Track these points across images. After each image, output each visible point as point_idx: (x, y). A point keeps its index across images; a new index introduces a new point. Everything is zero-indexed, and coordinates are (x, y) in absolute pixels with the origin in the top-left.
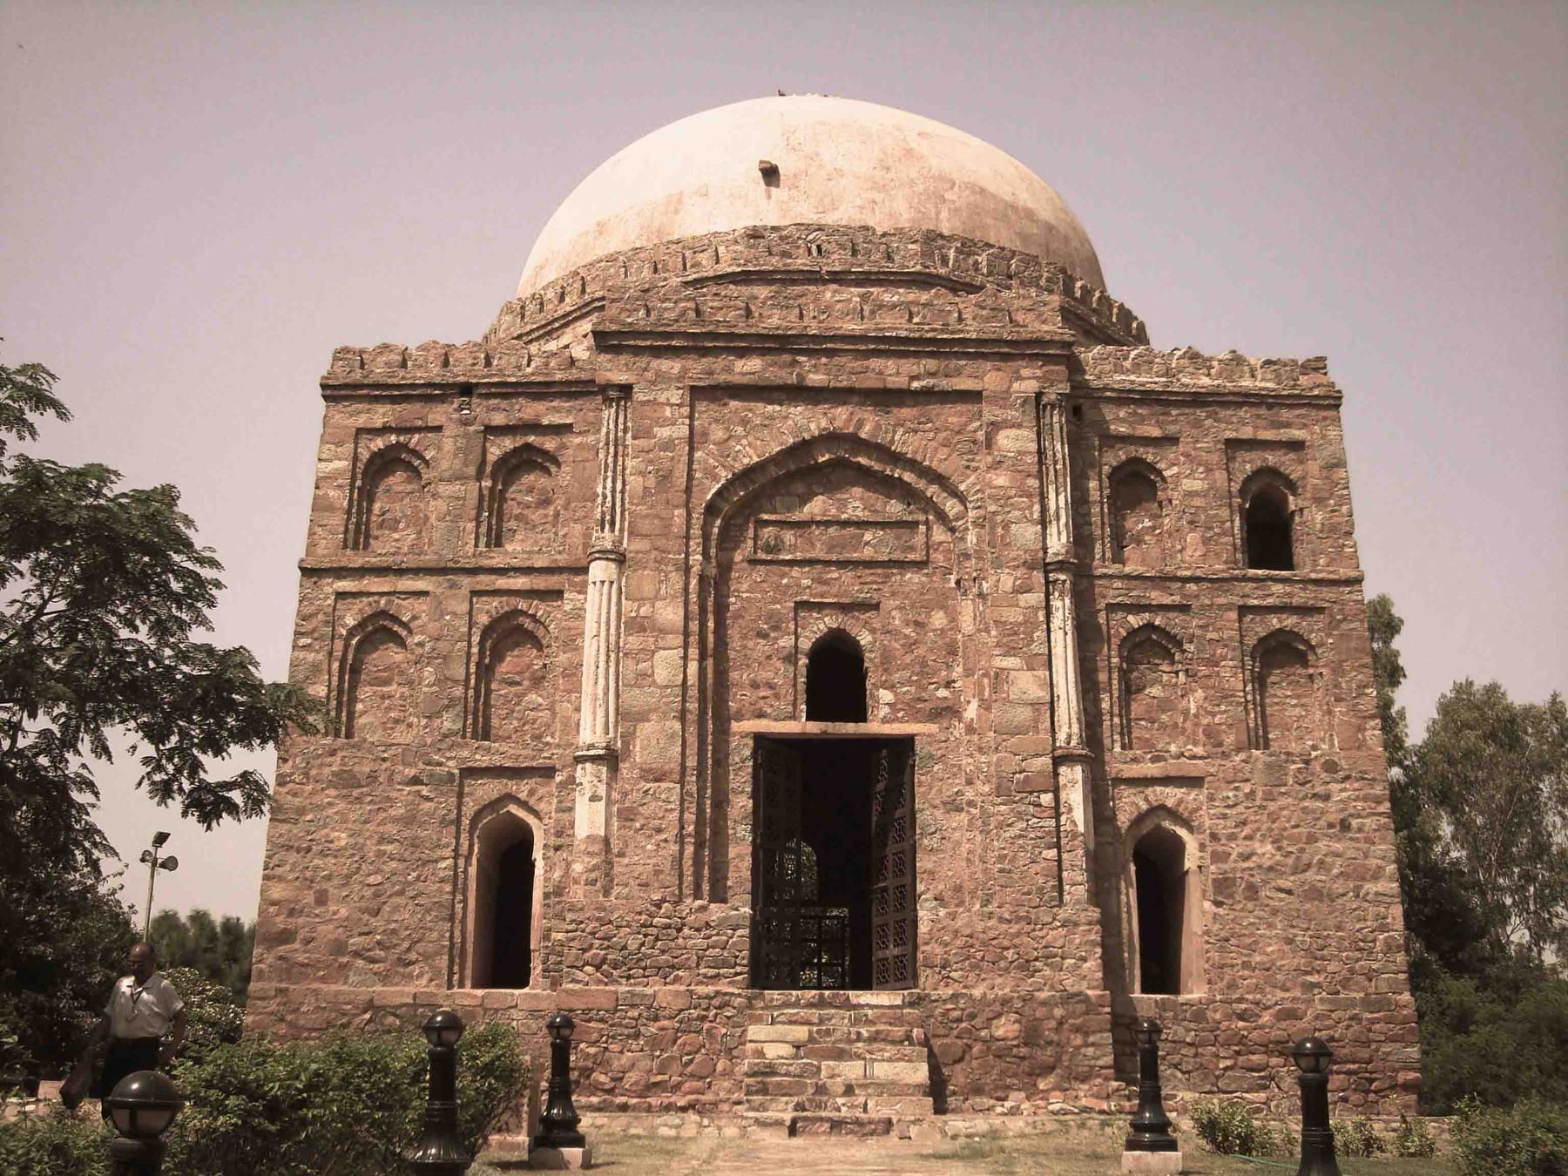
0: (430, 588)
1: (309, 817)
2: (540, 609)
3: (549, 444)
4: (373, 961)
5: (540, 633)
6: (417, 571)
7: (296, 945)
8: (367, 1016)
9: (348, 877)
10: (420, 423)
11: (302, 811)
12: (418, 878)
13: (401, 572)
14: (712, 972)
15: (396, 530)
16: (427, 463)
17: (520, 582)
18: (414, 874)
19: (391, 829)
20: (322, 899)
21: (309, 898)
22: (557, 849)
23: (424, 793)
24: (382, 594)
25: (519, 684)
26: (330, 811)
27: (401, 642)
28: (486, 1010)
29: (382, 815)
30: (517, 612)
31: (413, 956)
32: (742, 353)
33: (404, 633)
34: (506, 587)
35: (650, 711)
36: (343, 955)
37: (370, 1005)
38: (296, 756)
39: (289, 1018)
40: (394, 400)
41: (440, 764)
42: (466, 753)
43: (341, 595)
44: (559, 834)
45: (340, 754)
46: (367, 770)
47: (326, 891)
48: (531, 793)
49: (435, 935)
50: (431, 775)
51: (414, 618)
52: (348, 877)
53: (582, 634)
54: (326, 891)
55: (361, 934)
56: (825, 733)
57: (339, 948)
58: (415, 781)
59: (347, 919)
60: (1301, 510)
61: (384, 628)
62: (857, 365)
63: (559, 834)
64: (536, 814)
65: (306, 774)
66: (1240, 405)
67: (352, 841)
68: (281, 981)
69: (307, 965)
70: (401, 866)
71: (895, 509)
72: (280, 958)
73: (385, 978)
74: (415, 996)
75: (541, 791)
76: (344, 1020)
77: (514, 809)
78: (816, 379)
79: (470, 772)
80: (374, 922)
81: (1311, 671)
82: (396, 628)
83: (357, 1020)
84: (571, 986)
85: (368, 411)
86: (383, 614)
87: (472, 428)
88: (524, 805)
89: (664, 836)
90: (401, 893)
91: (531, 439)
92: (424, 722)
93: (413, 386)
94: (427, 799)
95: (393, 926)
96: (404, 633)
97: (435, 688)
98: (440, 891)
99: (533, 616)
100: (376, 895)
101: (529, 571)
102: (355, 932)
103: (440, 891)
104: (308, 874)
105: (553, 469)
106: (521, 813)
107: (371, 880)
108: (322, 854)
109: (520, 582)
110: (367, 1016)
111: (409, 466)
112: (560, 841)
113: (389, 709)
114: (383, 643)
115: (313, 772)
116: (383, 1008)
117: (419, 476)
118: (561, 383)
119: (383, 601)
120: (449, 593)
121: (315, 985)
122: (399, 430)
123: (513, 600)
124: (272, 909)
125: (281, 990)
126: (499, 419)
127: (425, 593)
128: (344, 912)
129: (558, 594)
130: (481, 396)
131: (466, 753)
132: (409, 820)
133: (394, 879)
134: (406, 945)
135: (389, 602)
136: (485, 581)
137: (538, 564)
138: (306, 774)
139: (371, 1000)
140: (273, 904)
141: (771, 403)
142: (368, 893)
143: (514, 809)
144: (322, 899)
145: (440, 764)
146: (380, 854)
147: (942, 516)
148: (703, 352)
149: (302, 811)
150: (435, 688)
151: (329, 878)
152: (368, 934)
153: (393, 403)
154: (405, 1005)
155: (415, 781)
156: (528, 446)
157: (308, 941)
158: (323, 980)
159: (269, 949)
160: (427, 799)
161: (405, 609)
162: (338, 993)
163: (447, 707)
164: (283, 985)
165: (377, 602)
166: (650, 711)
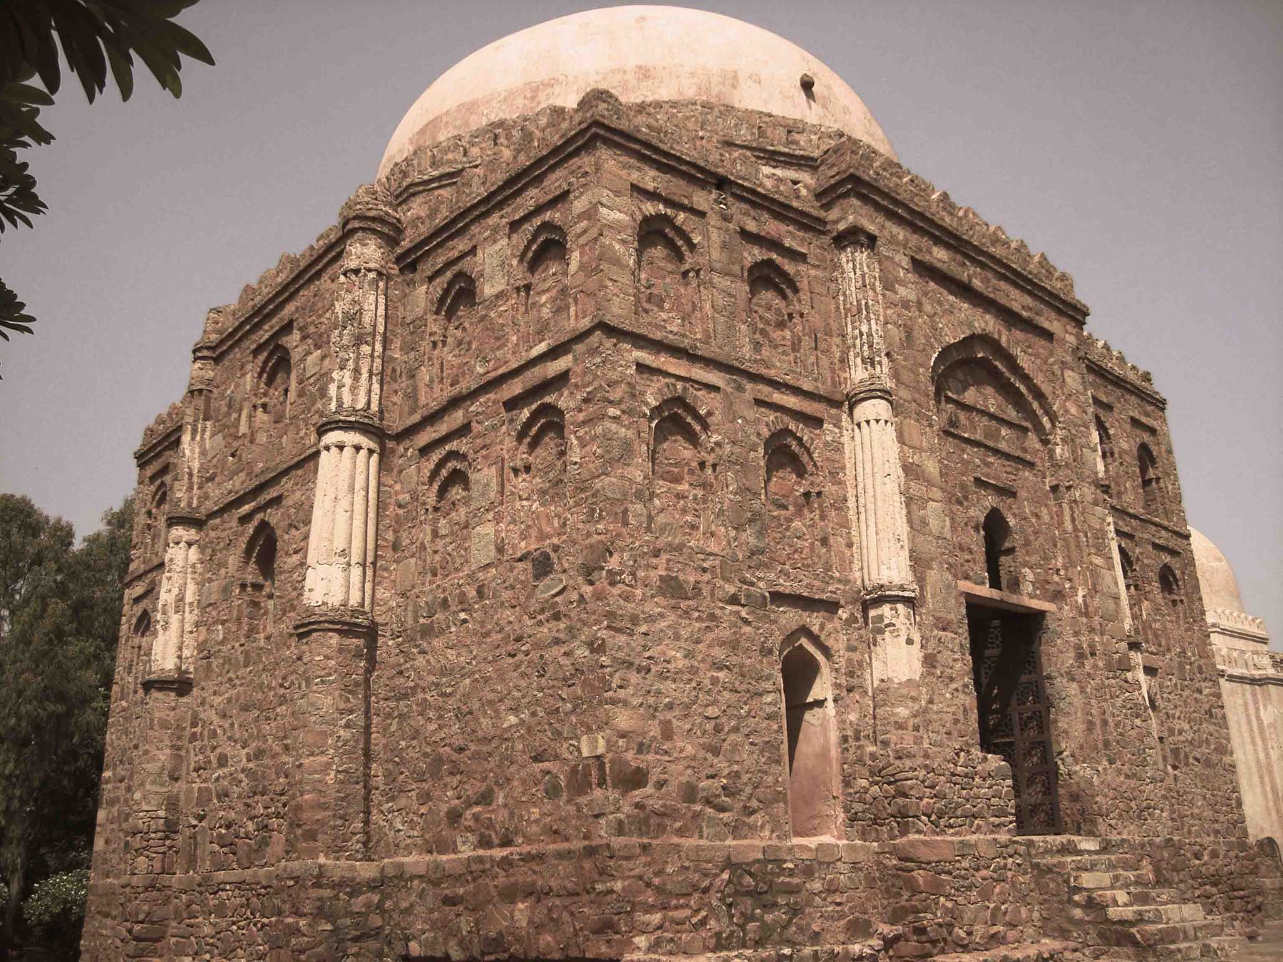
0: (721, 384)
1: (643, 629)
2: (805, 433)
3: (789, 267)
4: (722, 809)
5: (805, 459)
6: (710, 363)
7: (649, 789)
8: (725, 876)
9: (688, 707)
10: (686, 202)
11: (635, 620)
12: (750, 711)
13: (693, 358)
14: (997, 821)
15: (662, 309)
16: (692, 247)
17: (791, 401)
18: (746, 708)
19: (719, 653)
20: (668, 733)
21: (655, 730)
22: (850, 690)
23: (743, 614)
24: (679, 378)
25: (786, 508)
26: (663, 624)
27: (693, 439)
28: (820, 863)
29: (710, 636)
30: (787, 432)
31: (754, 804)
32: (937, 241)
33: (698, 428)
34: (782, 403)
35: (932, 559)
36: (694, 802)
37: (729, 864)
38: (623, 550)
39: (656, 881)
40: (661, 167)
41: (752, 584)
42: (772, 576)
43: (641, 367)
44: (851, 674)
45: (664, 557)
46: (692, 579)
47: (670, 722)
48: (822, 627)
49: (770, 779)
50: (748, 596)
51: (710, 414)
52: (688, 707)
53: (843, 468)
54: (670, 722)
55: (708, 777)
56: (1002, 601)
57: (690, 793)
58: (734, 600)
59: (694, 758)
60: (1158, 479)
61: (675, 419)
62: (994, 281)
63: (851, 674)
64: (826, 651)
65: (633, 574)
66: (1132, 393)
67: (687, 663)
68: (641, 835)
69: (664, 814)
70: (734, 697)
71: (1012, 414)
72: (638, 806)
73: (736, 830)
74: (764, 852)
75: (829, 626)
76: (706, 883)
77: (804, 642)
78: (977, 283)
79: (779, 598)
80: (721, 764)
81: (1176, 597)
82: (689, 420)
83: (718, 882)
84: (917, 836)
85: (639, 169)
86: (679, 400)
87: (731, 226)
88: (815, 639)
89: (954, 686)
90: (736, 730)
91: (775, 256)
92: (733, 533)
93: (679, 159)
94: (746, 622)
95: (736, 768)
96: (698, 428)
97: (738, 498)
98: (768, 728)
99: (800, 440)
100: (718, 729)
101: (797, 391)
102: (703, 775)
103: (768, 728)
104: (651, 700)
105: (789, 292)
106: (811, 648)
107: (711, 711)
108: (662, 676)
109: (791, 401)
110: (725, 876)
111: (670, 244)
112: (855, 681)
113: (684, 511)
114: (672, 434)
115: (641, 574)
116: (739, 865)
117: (680, 258)
118: (796, 210)
119: (680, 385)
120: (736, 393)
121: (676, 840)
122: (668, 202)
123: (786, 419)
124: (621, 742)
125: (645, 848)
126: (751, 226)
127: (716, 389)
128: (690, 750)
129: (817, 422)
130: (733, 195)
131: (772, 576)
132: (734, 645)
133: (729, 712)
134: (748, 790)
135: (685, 389)
136: (765, 391)
137: (806, 387)
138: (633, 574)
139: (729, 858)
140: (623, 736)
141: (951, 293)
142: (709, 726)
143: (804, 642)
144: (668, 733)
145: (752, 584)
146: (715, 681)
147: (1039, 428)
148: (916, 229)
149: (635, 620)
150: (738, 498)
151: (670, 707)
152: (713, 777)
153: (658, 169)
154: (758, 861)
155: (734, 600)
156: (770, 263)
157: (660, 785)
158: (680, 832)
159: (624, 794)
160: (746, 622)
161: (705, 403)
162: (698, 849)
163: (750, 521)
164: (646, 841)
165: (674, 386)
166: (932, 559)
